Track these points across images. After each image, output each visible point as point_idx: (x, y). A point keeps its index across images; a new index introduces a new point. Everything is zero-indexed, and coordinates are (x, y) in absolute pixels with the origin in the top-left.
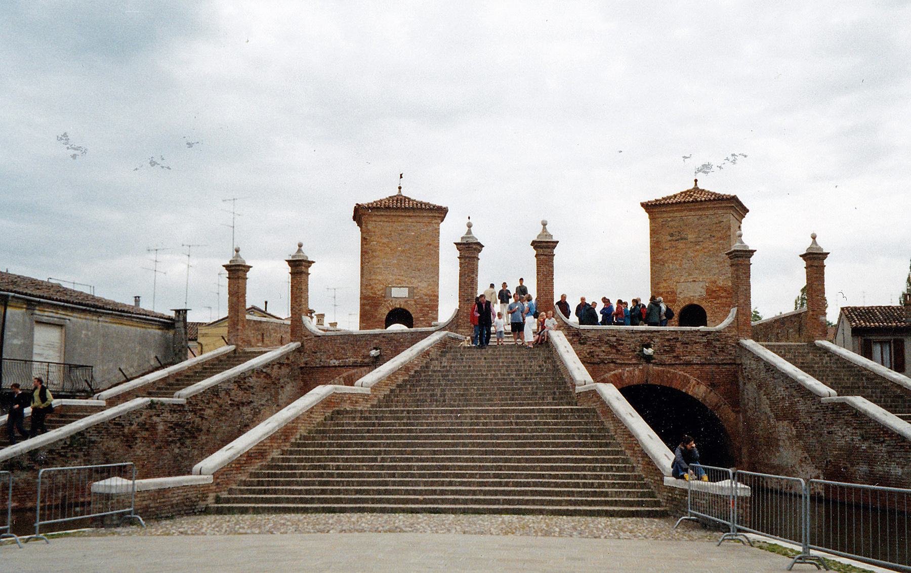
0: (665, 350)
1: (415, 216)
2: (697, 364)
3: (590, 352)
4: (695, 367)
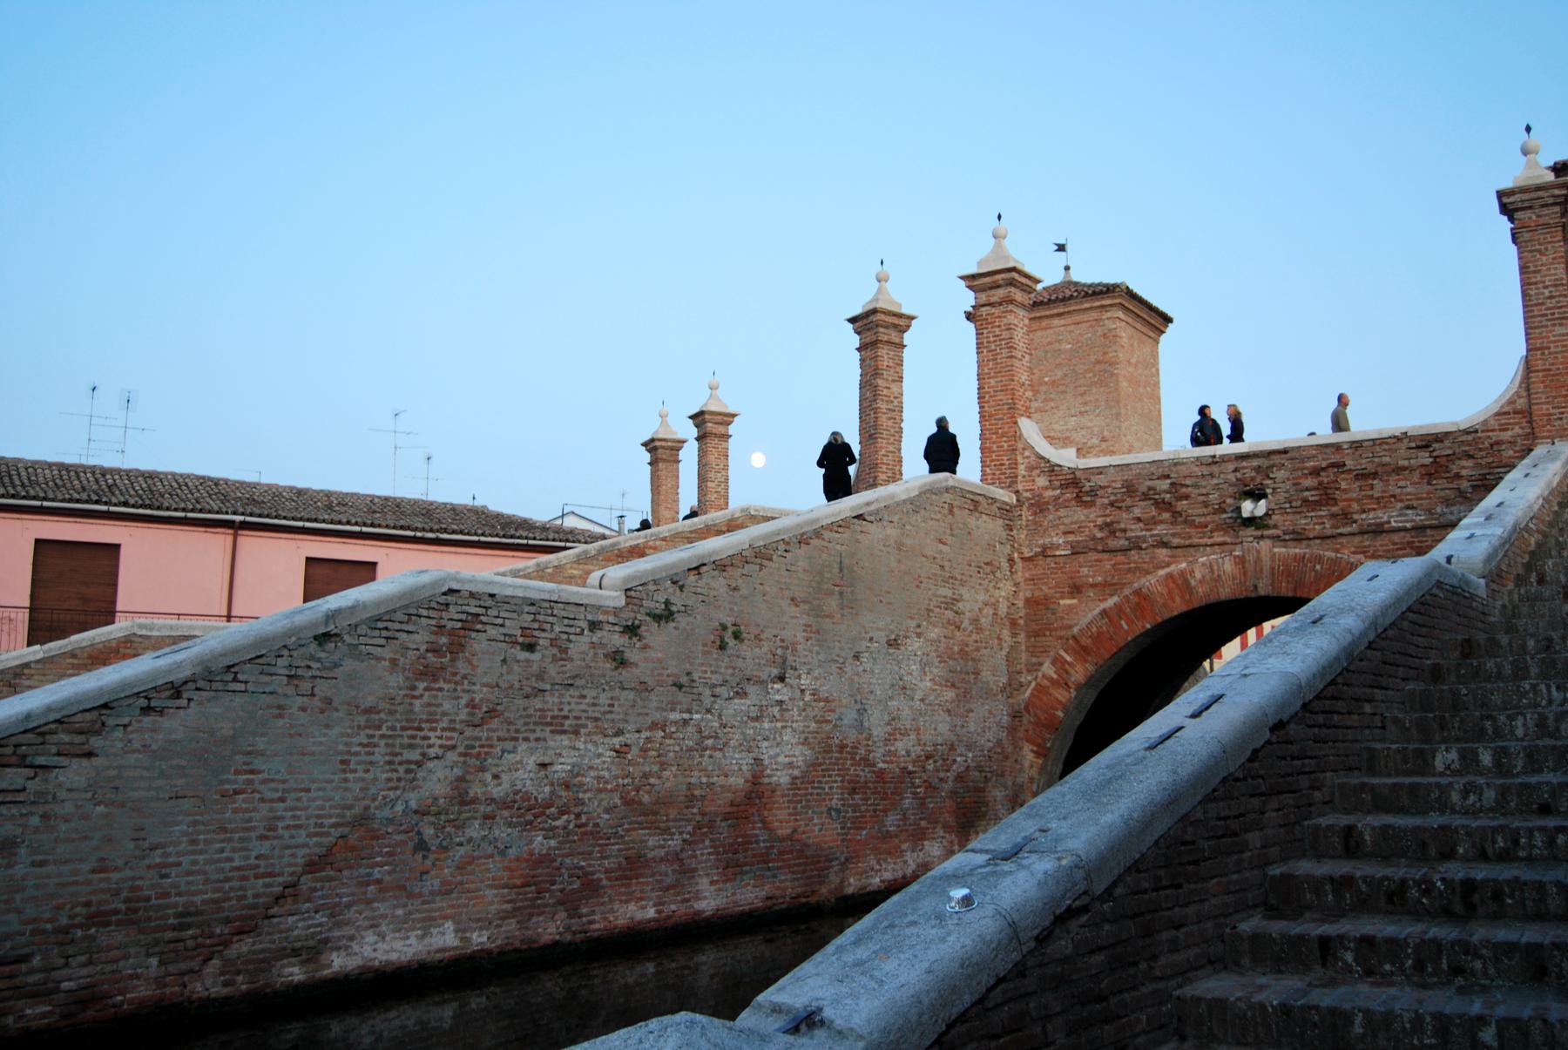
0: (1305, 501)
1: (1069, 312)
2: (1405, 529)
3: (1107, 525)
4: (1396, 537)
